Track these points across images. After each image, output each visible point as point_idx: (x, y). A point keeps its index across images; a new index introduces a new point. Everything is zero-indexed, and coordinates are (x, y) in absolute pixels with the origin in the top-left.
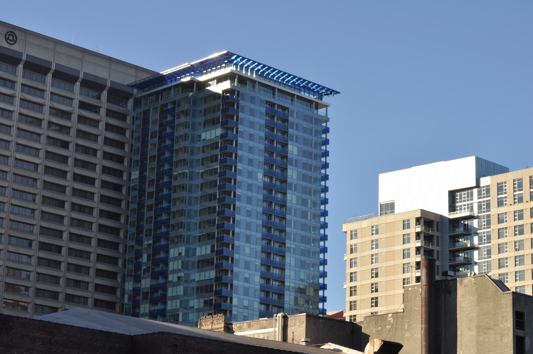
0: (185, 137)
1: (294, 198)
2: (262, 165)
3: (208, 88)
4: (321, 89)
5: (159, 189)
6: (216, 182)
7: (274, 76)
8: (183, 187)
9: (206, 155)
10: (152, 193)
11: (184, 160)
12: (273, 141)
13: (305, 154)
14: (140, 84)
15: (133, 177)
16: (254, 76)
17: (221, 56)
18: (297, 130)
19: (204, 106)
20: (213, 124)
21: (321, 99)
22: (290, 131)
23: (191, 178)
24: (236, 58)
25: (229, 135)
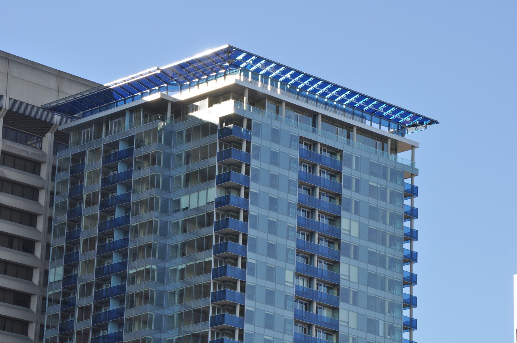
0: (150, 204)
1: (353, 317)
2: (292, 256)
3: (194, 114)
4: (403, 116)
5: (101, 301)
6: (207, 287)
7: (315, 91)
8: (146, 298)
9: (189, 237)
10: (88, 308)
11: (149, 246)
12: (313, 211)
13: (372, 280)
14: (65, 105)
15: (51, 279)
16: (279, 91)
17: (217, 54)
18: (357, 190)
19: (185, 147)
20: (203, 179)
21: (403, 135)
22: (345, 193)
23: (161, 280)
24: (245, 59)
25: (232, 199)
